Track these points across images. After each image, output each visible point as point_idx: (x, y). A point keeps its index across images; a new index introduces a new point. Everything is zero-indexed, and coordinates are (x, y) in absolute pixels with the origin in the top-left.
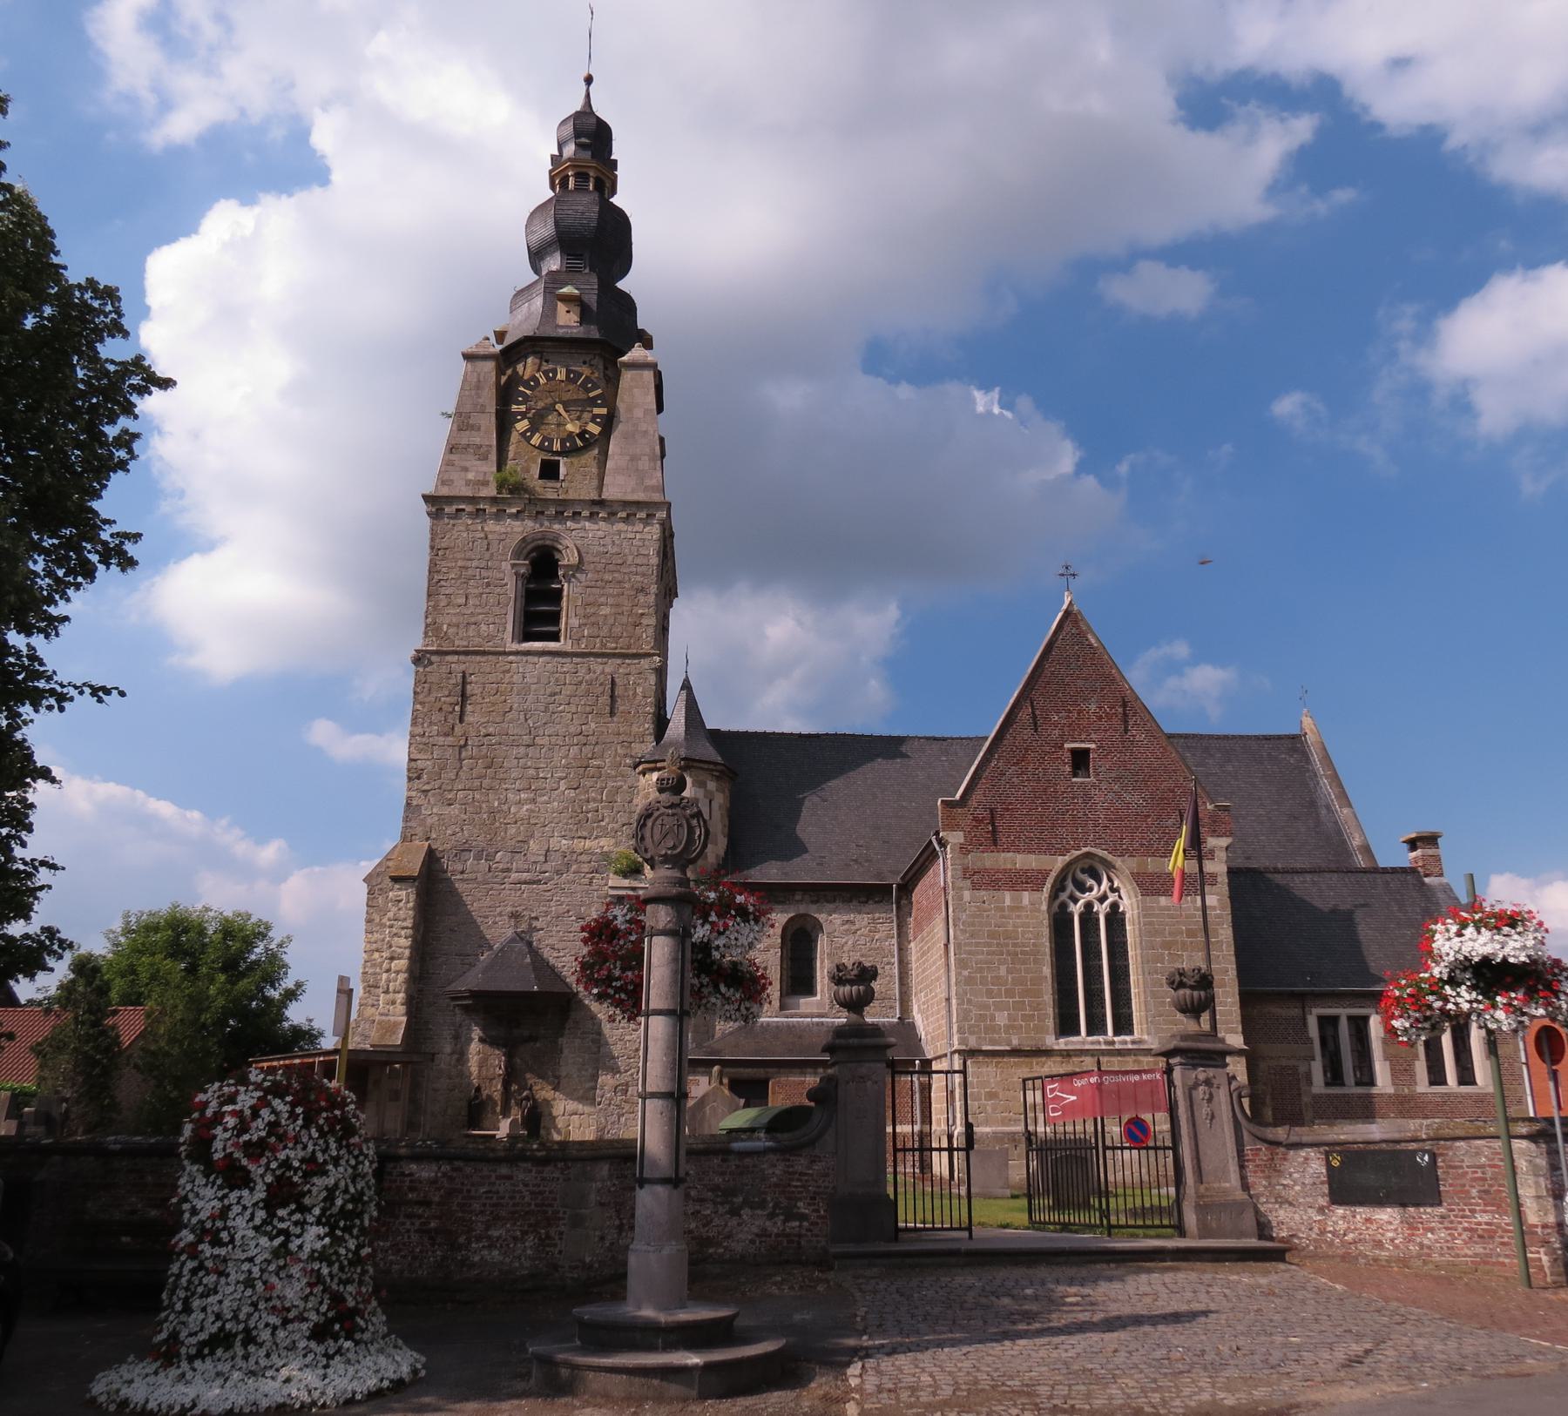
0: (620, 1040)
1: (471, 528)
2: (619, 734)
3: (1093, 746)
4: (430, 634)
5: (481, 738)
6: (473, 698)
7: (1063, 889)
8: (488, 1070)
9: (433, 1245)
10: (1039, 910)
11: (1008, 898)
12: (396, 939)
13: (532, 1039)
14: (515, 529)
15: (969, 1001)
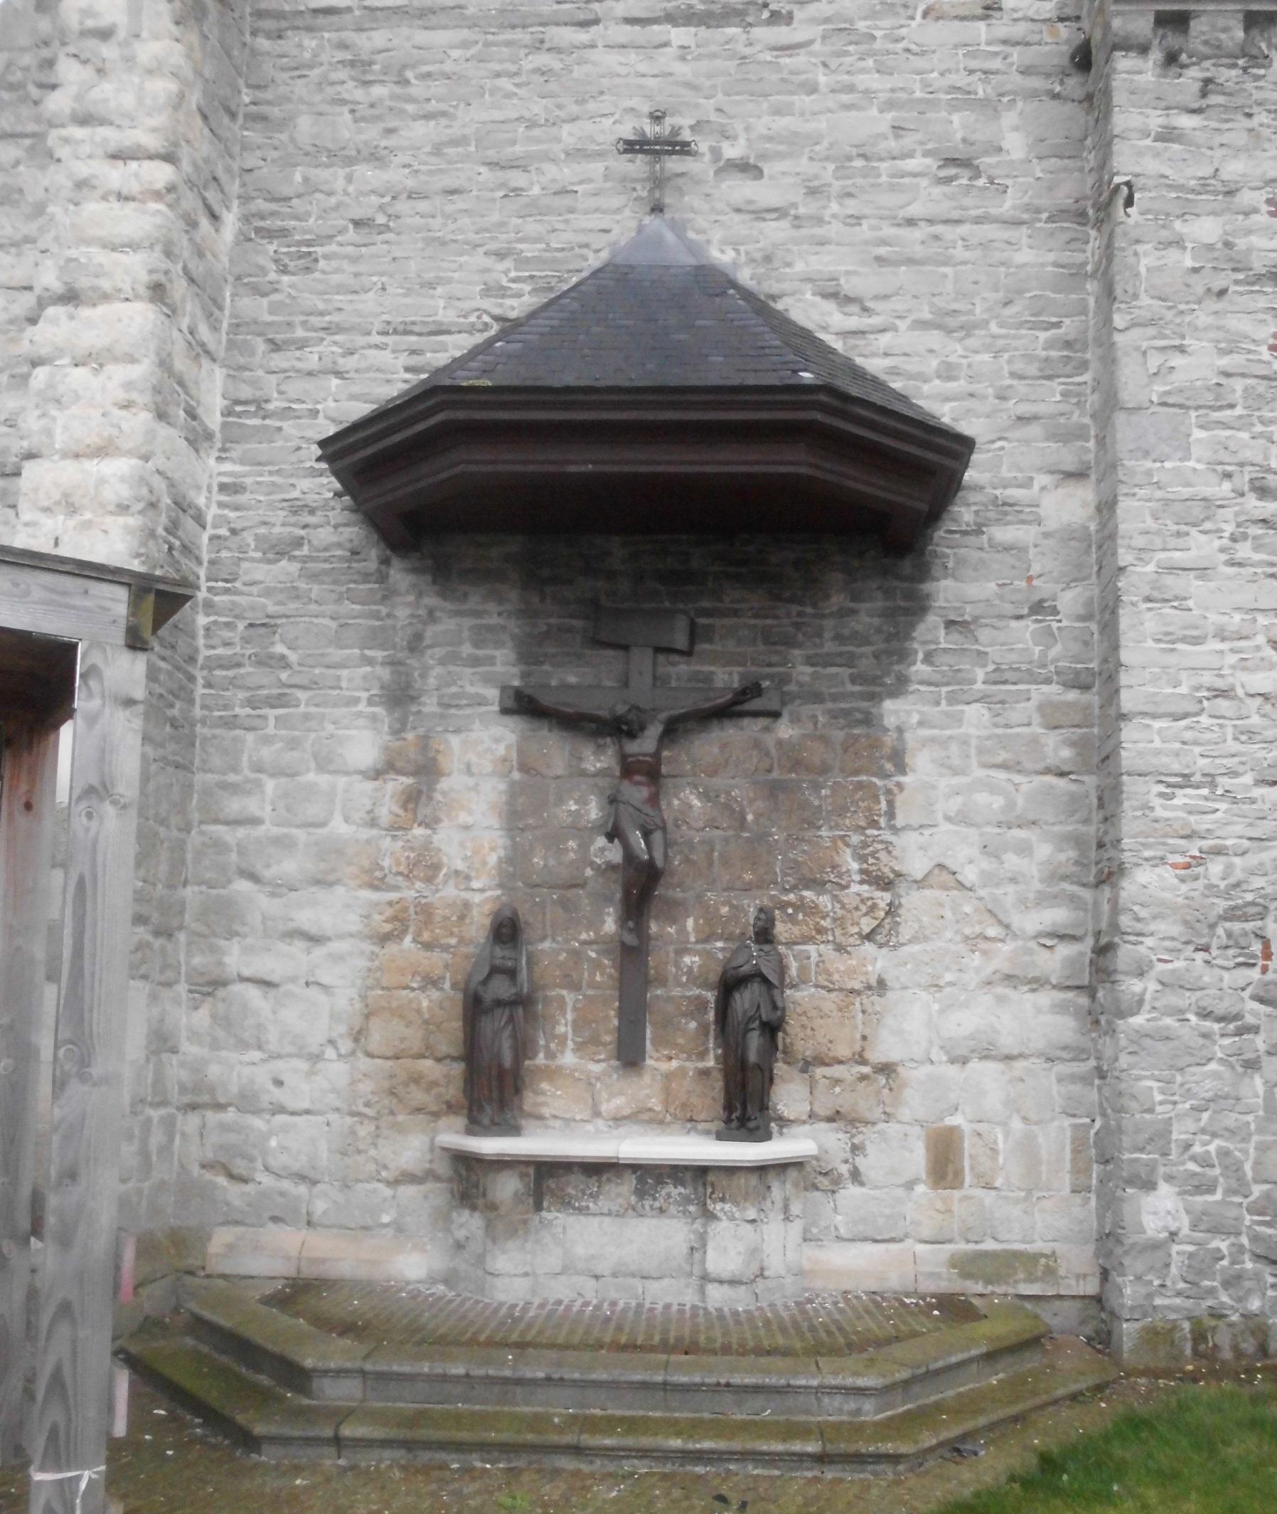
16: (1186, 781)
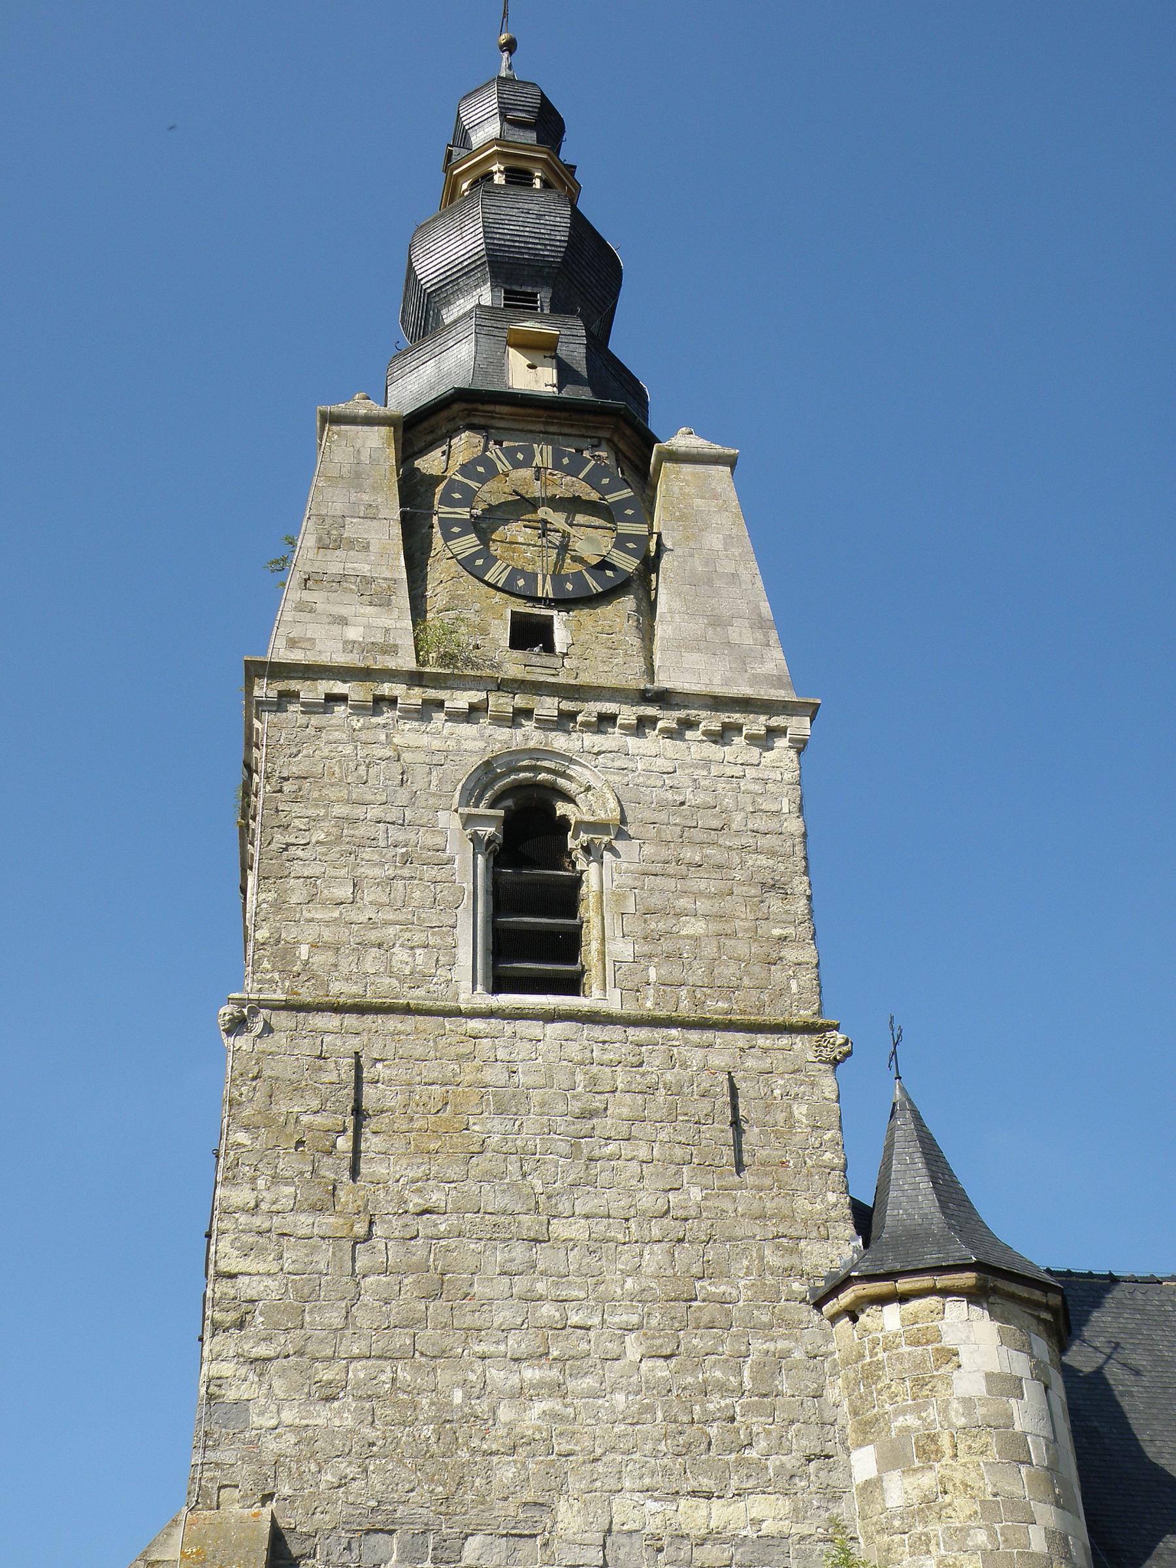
1: (363, 736)
2: (763, 1216)
4: (266, 965)
5: (408, 1219)
6: (385, 1118)
14: (468, 745)
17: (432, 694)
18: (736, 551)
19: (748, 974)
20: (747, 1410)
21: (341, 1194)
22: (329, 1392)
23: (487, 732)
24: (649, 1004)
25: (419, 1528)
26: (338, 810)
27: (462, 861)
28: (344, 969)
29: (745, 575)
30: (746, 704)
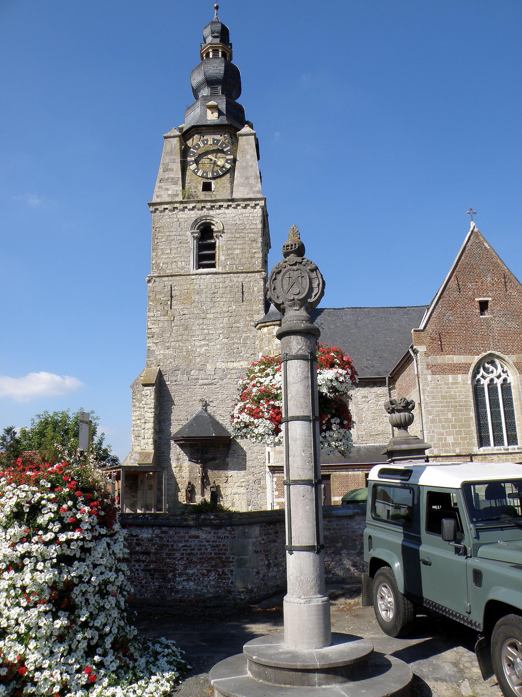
0: (256, 458)
1: (172, 216)
2: (247, 311)
3: (490, 299)
4: (154, 268)
5: (181, 316)
7: (478, 372)
8: (194, 474)
9: (153, 579)
10: (467, 384)
11: (450, 378)
12: (147, 413)
13: (214, 459)
15: (433, 431)
16: (253, 467)
17: (185, 205)
18: (253, 159)
19: (247, 261)
20: (241, 347)
21: (168, 312)
22: (168, 348)
23: (196, 212)
24: (227, 269)
25: (183, 370)
26: (167, 234)
27: (191, 242)
28: (169, 268)
29: (254, 165)
30: (250, 199)
